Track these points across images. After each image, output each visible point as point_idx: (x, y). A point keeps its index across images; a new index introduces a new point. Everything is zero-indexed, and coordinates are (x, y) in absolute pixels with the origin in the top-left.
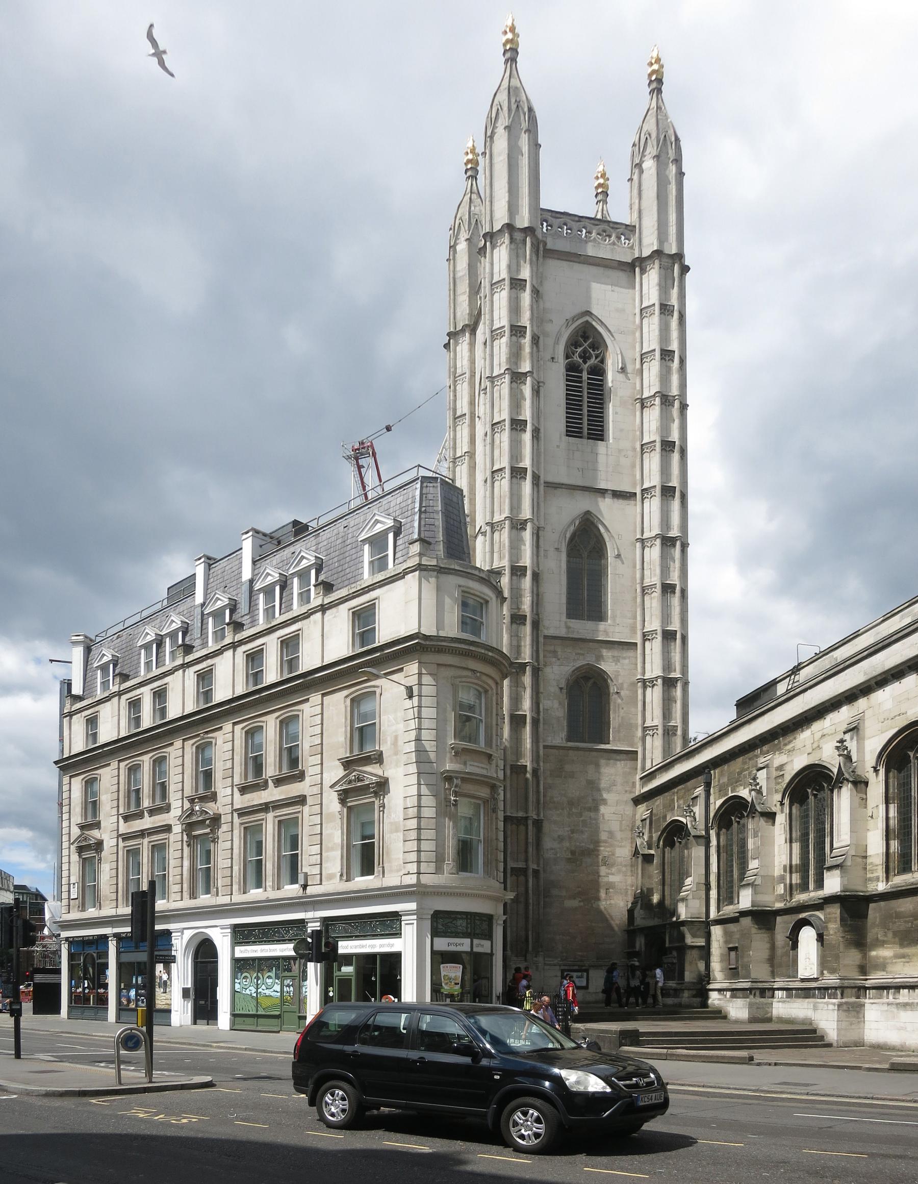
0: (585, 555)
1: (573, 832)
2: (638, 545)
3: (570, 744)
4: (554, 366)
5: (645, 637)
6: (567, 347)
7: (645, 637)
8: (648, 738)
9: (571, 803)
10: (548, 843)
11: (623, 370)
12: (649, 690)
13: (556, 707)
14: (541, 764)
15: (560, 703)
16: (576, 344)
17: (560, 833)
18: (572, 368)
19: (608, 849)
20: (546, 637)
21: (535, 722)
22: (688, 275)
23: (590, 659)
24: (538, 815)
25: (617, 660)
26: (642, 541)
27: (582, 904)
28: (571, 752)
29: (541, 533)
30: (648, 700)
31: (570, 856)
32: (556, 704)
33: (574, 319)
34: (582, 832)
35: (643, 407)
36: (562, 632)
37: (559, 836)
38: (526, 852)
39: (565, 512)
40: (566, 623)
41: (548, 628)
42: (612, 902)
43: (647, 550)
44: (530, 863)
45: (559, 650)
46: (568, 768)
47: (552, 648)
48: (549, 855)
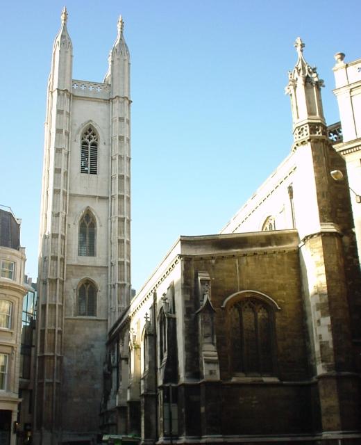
3: (78, 317)
4: (76, 143)
6: (82, 134)
8: (112, 314)
12: (112, 289)
13: (73, 298)
16: (86, 134)
18: (85, 143)
20: (67, 265)
21: (61, 307)
23: (88, 276)
33: (85, 124)
36: (75, 262)
39: (79, 208)
46: (76, 329)
47: (71, 270)
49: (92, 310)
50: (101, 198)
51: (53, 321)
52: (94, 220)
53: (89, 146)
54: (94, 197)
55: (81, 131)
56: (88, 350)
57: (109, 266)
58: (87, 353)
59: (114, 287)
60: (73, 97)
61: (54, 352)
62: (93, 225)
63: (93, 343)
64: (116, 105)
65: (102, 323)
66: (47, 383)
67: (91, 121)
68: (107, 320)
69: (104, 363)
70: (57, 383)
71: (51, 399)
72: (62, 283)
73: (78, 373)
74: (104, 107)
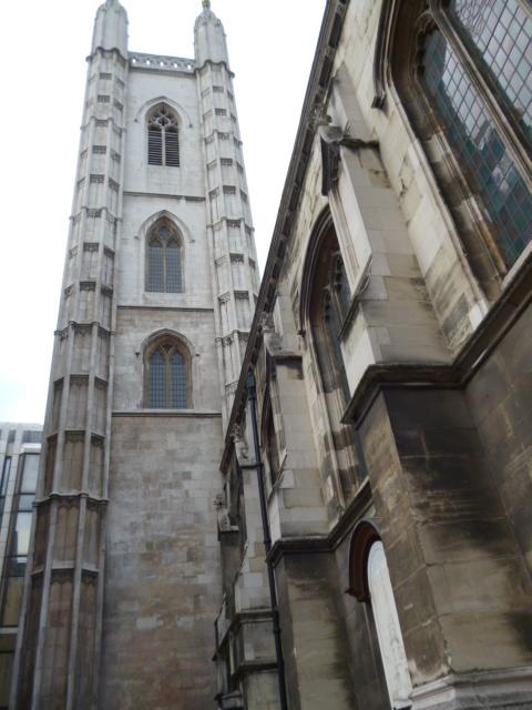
0: (164, 244)
1: (149, 516)
2: (210, 230)
4: (136, 125)
5: (221, 302)
7: (221, 302)
9: (147, 480)
10: (117, 534)
11: (191, 126)
13: (130, 372)
14: (109, 432)
15: (136, 369)
16: (157, 116)
17: (133, 520)
18: (153, 130)
19: (195, 538)
20: (119, 307)
22: (234, 81)
23: (169, 326)
24: (101, 495)
25: (196, 325)
26: (212, 227)
27: (161, 623)
28: (147, 419)
29: (118, 223)
30: (227, 358)
31: (145, 551)
32: (131, 370)
34: (161, 516)
35: (206, 143)
37: (132, 524)
38: (76, 545)
39: (142, 214)
40: (144, 295)
41: (126, 300)
42: (204, 616)
43: (217, 234)
44: (79, 560)
45: (136, 318)
46: (144, 437)
47: (129, 317)
48: (116, 552)
49: (182, 392)
50: (189, 199)
51: (81, 414)
52: (177, 232)
53: (163, 132)
54: (178, 198)
55: (147, 109)
56: (178, 485)
57: (216, 307)
58: (174, 492)
59: (230, 342)
60: (132, 69)
61: (79, 485)
62: (175, 241)
63: (187, 468)
64: (207, 80)
65: (208, 421)
66: (54, 572)
67: (163, 97)
68: (219, 415)
69: (220, 505)
70: (85, 573)
71: (65, 621)
72: (105, 335)
73: (149, 546)
74: (188, 82)
